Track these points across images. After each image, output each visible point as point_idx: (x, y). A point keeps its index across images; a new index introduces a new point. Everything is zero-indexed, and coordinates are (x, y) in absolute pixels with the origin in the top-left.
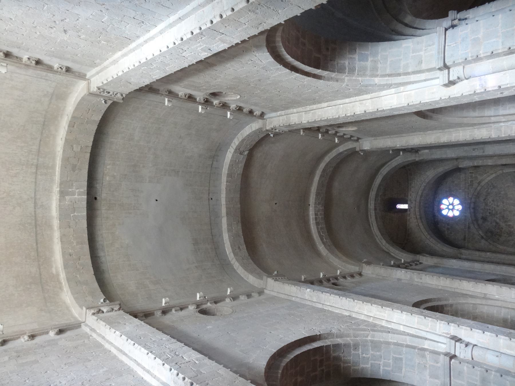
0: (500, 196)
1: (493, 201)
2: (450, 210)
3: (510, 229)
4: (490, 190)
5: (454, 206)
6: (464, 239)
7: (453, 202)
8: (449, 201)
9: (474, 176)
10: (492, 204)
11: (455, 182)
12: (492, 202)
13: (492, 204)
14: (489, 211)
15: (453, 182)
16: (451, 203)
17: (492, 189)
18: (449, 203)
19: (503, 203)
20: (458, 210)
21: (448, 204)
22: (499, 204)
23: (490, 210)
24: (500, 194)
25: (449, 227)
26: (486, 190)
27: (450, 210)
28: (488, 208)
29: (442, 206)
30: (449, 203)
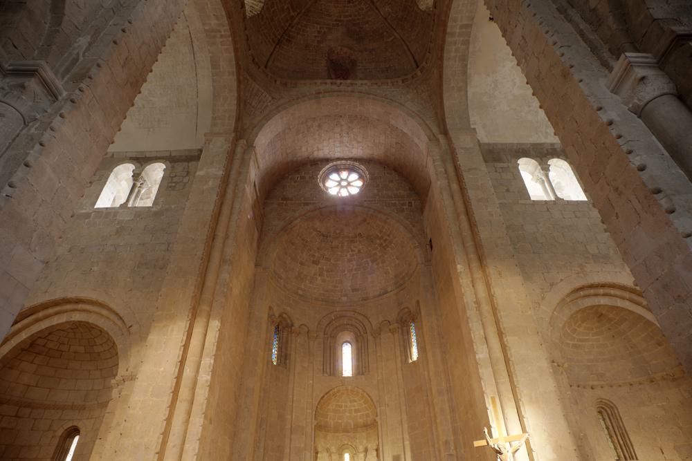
0: (368, 264)
1: (359, 251)
2: (337, 183)
3: (309, 278)
4: (378, 241)
5: (346, 187)
6: (285, 199)
7: (352, 186)
8: (356, 180)
9: (405, 207)
10: (352, 251)
11: (391, 185)
12: (357, 250)
13: (352, 251)
14: (340, 245)
15: (392, 181)
16: (351, 184)
17: (381, 245)
18: (352, 182)
19: (355, 269)
20: (339, 192)
21: (350, 180)
22: (354, 263)
23: (342, 247)
24: (373, 261)
25: (307, 179)
26: (379, 234)
27: (337, 183)
28: (346, 244)
29: (344, 174)
30: (352, 182)
